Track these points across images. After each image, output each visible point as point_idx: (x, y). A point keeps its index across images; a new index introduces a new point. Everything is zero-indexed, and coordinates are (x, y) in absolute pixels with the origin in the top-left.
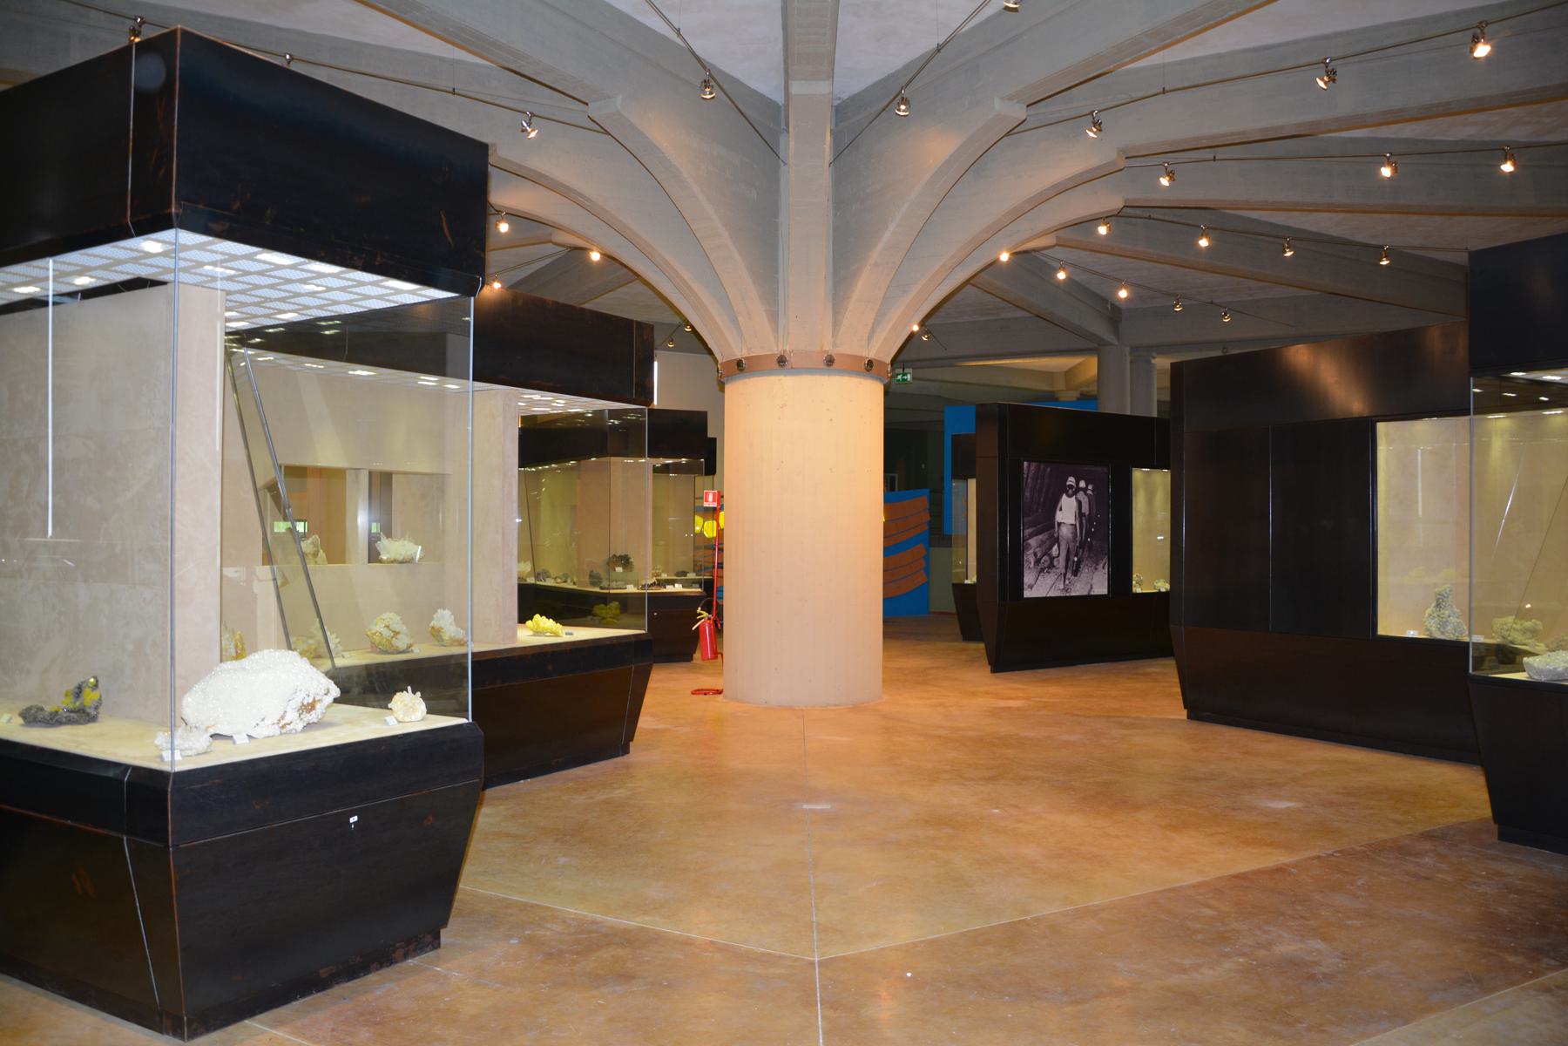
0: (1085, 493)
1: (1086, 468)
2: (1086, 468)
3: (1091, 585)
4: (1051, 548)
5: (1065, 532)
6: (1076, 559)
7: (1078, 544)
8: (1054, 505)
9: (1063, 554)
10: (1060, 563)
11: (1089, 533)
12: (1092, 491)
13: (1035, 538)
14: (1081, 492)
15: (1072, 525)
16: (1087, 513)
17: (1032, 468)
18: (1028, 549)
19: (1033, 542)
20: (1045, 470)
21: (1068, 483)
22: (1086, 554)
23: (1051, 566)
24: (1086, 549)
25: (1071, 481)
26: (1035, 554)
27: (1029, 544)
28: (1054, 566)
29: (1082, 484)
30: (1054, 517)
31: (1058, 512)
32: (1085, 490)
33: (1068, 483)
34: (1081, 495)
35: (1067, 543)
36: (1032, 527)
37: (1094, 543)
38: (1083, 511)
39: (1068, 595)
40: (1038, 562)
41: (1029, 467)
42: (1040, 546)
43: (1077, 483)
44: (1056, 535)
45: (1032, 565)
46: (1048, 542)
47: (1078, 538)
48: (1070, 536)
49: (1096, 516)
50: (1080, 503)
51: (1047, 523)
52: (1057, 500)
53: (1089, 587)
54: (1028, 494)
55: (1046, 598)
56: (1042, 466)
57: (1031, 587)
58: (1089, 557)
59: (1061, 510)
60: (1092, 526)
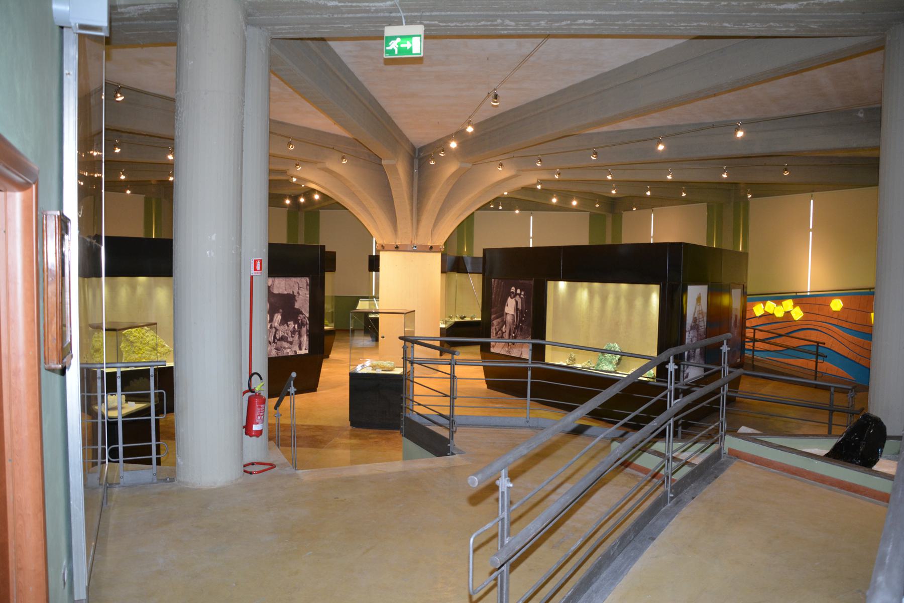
0: (520, 297)
1: (521, 282)
2: (521, 282)
3: (522, 352)
4: (502, 327)
5: (509, 319)
6: (514, 335)
7: (515, 326)
8: (504, 303)
9: (508, 331)
10: (506, 335)
11: (521, 321)
12: (524, 295)
13: (496, 320)
14: (518, 296)
15: (512, 315)
16: (520, 309)
17: (496, 282)
18: (493, 326)
19: (495, 322)
20: (501, 283)
21: (512, 291)
22: (519, 333)
23: (502, 337)
24: (519, 330)
25: (513, 289)
26: (496, 330)
27: (493, 323)
28: (503, 337)
29: (518, 291)
30: (504, 310)
31: (506, 307)
32: (520, 295)
33: (512, 291)
34: (517, 298)
35: (510, 325)
36: (496, 314)
37: (523, 327)
38: (518, 307)
39: (510, 355)
40: (497, 333)
41: (494, 282)
42: (498, 325)
43: (516, 291)
44: (505, 320)
45: (494, 335)
46: (501, 324)
47: (515, 323)
48: (511, 321)
49: (525, 311)
50: (517, 302)
51: (502, 314)
52: (506, 300)
53: (520, 353)
54: (493, 296)
55: (499, 354)
56: (500, 281)
57: (494, 347)
58: (520, 335)
59: (507, 306)
60: (523, 317)
